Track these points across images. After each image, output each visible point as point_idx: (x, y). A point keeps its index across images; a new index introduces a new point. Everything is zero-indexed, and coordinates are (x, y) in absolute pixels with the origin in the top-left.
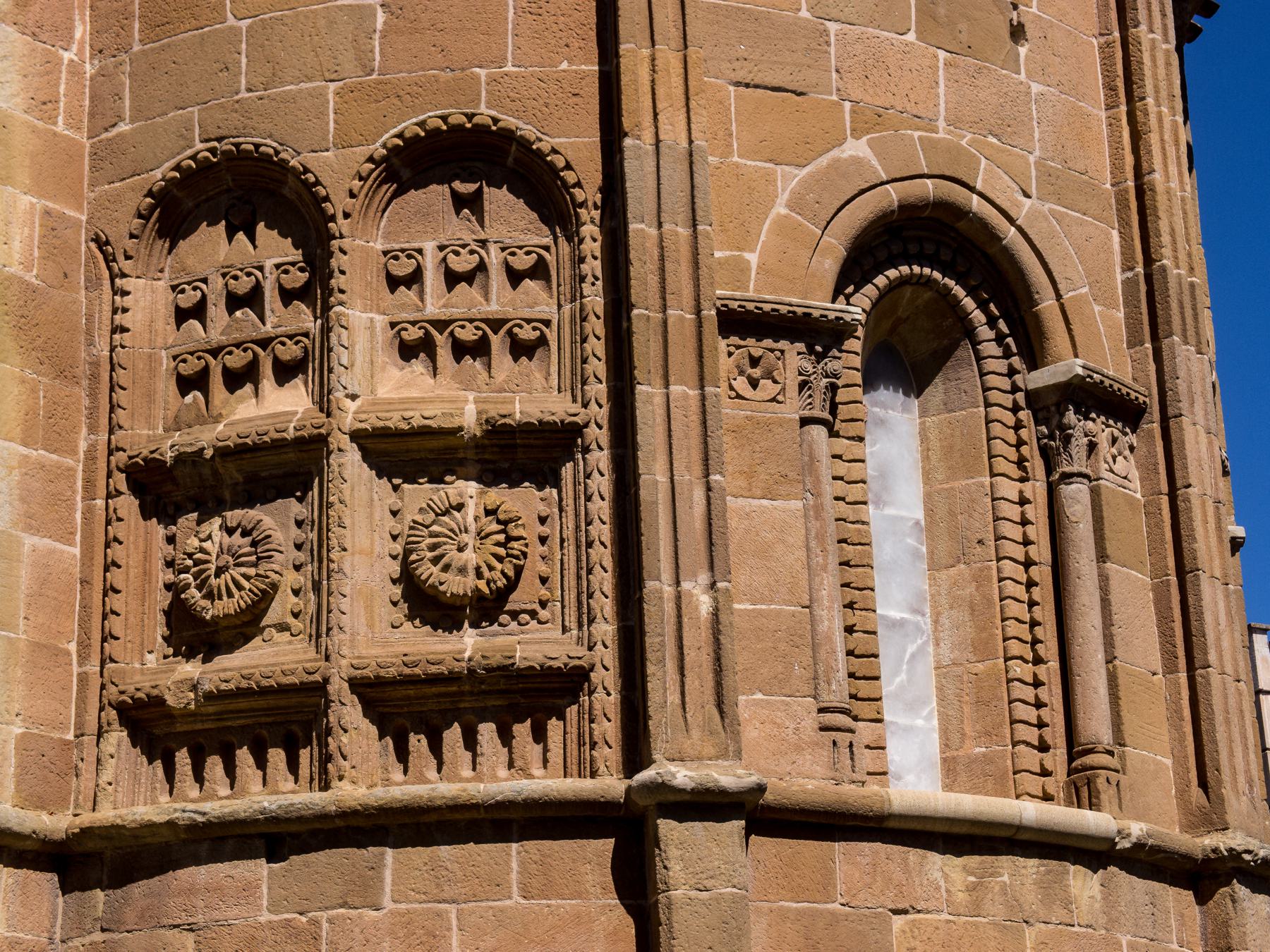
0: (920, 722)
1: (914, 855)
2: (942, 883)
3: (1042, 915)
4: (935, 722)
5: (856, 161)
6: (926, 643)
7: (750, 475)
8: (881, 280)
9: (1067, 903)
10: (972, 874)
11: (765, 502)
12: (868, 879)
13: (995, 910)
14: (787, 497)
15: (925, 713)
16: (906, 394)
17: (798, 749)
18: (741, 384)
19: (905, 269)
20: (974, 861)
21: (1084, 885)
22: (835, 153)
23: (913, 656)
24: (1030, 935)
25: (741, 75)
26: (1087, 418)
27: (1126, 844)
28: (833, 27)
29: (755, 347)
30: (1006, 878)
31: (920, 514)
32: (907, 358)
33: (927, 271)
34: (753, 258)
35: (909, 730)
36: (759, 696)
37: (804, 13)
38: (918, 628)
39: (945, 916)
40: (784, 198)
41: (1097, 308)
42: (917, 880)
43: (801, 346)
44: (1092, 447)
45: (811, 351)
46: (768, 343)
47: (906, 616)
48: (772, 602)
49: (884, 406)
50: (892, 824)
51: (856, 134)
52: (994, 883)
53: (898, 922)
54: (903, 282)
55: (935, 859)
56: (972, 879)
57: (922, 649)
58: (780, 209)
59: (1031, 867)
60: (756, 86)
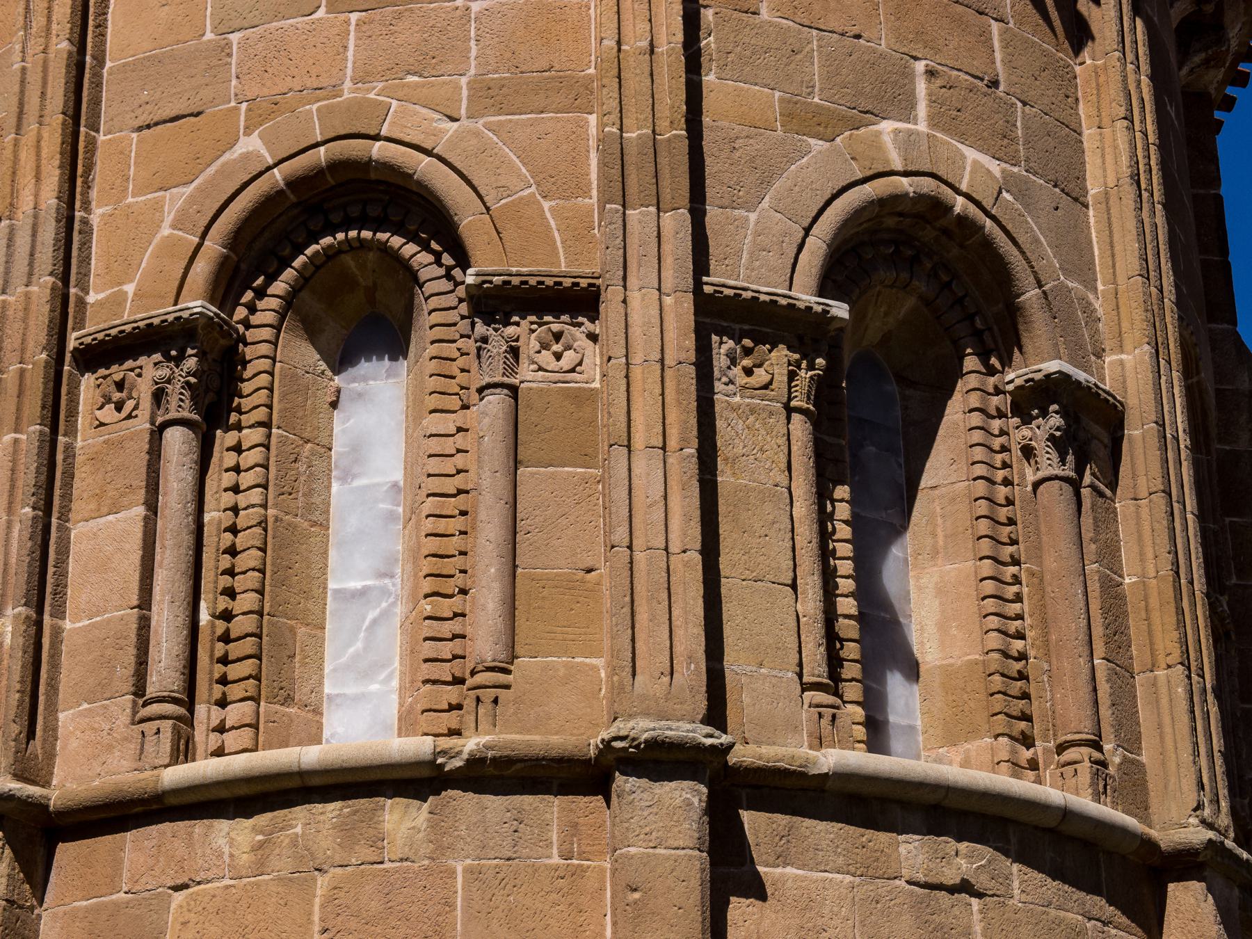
0: (374, 687)
1: (199, 827)
2: (226, 850)
3: (338, 860)
4: (395, 683)
5: (246, 157)
6: (394, 604)
7: (99, 497)
8: (299, 261)
9: (377, 841)
10: (261, 832)
11: (110, 518)
12: (151, 862)
13: (281, 863)
14: (127, 508)
15: (382, 676)
16: (393, 358)
17: (110, 748)
18: (108, 414)
19: (328, 240)
20: (263, 819)
21: (401, 819)
22: (227, 157)
23: (375, 622)
24: (322, 882)
25: (144, 119)
26: (507, 323)
27: (458, 763)
28: (235, 38)
29: (117, 372)
30: (299, 830)
31: (398, 476)
32: (365, 323)
33: (353, 234)
34: (130, 288)
35: (358, 698)
36: (86, 706)
37: (209, 36)
38: (385, 592)
39: (227, 882)
40: (169, 219)
41: (546, 205)
42: (199, 852)
43: (157, 357)
44: (515, 352)
45: (168, 358)
46: (130, 364)
47: (369, 583)
48: (105, 611)
49: (365, 379)
50: (173, 801)
51: (248, 131)
52: (284, 838)
53: (179, 897)
54: (331, 254)
55: (222, 826)
56: (260, 837)
57: (385, 614)
58: (166, 231)
59: (332, 810)
60: (156, 124)
